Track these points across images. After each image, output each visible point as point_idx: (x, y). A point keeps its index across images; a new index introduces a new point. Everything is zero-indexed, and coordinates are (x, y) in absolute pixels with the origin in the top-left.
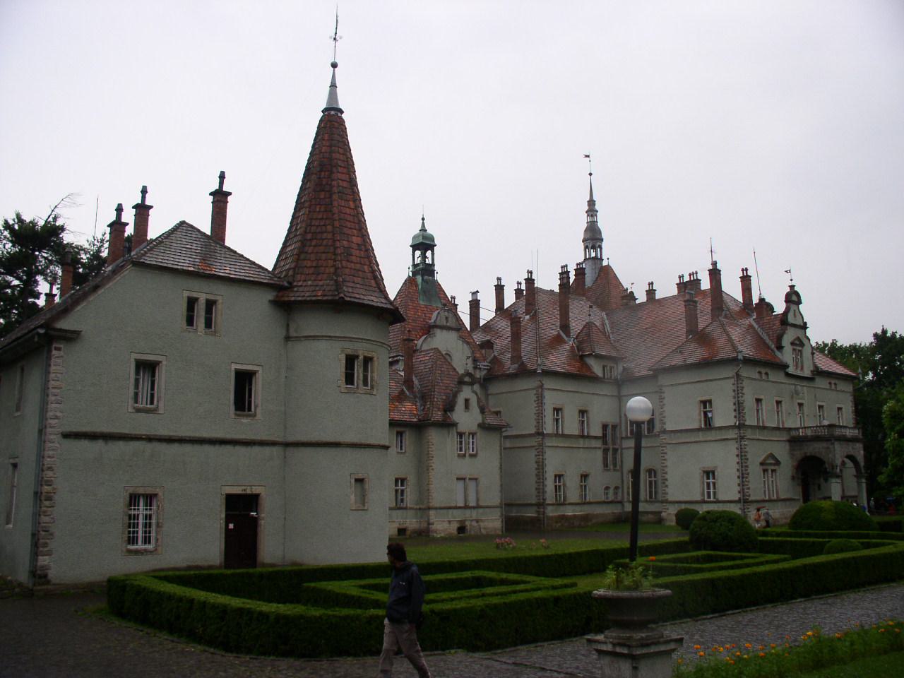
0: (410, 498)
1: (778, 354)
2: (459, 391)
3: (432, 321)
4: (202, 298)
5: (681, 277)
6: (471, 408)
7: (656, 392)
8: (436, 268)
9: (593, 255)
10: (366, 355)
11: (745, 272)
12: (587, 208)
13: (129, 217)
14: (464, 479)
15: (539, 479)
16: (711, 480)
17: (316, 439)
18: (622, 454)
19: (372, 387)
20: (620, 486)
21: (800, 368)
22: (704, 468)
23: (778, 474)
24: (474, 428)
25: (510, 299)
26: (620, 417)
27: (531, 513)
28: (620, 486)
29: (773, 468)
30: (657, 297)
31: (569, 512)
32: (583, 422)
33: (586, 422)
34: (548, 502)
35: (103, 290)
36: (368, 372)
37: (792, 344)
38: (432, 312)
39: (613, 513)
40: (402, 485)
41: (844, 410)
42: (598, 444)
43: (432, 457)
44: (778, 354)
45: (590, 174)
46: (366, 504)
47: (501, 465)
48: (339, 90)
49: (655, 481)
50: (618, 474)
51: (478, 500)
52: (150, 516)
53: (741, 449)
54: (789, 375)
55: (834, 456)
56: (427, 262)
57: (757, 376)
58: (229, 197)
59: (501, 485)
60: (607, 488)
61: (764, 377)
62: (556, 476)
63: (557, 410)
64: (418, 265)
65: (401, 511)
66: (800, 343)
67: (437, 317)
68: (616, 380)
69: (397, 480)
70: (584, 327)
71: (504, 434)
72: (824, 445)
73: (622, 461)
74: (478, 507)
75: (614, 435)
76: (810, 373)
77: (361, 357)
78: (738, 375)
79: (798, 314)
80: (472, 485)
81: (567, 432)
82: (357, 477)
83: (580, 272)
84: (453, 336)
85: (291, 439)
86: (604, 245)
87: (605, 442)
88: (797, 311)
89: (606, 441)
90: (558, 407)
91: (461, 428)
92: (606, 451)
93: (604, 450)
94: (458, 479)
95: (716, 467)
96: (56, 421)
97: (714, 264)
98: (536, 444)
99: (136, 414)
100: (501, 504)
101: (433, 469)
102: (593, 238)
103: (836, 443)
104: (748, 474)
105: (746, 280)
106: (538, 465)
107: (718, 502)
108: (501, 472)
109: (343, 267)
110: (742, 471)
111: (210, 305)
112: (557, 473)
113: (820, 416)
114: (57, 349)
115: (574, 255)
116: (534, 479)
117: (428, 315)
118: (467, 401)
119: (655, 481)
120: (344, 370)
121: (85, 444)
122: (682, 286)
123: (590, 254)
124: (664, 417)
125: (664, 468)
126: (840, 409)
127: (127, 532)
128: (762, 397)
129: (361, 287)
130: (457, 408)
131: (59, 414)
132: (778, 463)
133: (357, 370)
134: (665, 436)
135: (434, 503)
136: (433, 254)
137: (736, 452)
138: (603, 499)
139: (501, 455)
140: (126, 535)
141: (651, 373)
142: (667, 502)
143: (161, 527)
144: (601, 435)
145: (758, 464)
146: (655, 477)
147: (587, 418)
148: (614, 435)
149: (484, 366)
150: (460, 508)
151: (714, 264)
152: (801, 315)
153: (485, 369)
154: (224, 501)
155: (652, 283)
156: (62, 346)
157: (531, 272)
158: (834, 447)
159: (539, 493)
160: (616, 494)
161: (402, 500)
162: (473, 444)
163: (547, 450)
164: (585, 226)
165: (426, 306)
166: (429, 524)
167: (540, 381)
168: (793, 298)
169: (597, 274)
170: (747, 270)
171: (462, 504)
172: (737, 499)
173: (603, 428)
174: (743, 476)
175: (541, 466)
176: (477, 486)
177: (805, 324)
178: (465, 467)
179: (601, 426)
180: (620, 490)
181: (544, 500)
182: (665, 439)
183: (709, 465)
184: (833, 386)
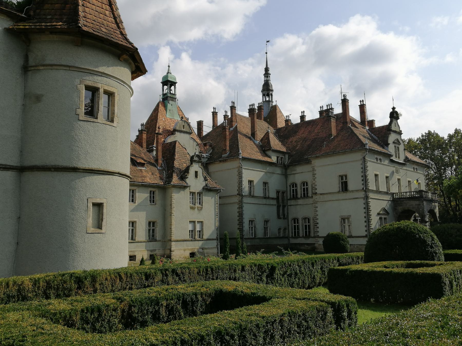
7: (309, 172)
9: (267, 99)
11: (362, 102)
12: (264, 72)
14: (194, 222)
15: (240, 222)
17: (53, 164)
18: (288, 209)
20: (287, 228)
21: (397, 157)
22: (342, 216)
28: (287, 228)
29: (385, 216)
32: (265, 189)
37: (394, 142)
40: (153, 226)
42: (275, 202)
45: (266, 53)
49: (309, 226)
50: (286, 220)
55: (423, 210)
60: (279, 229)
62: (250, 221)
63: (250, 182)
64: (166, 94)
65: (152, 243)
66: (397, 142)
69: (150, 223)
70: (266, 134)
72: (417, 202)
73: (288, 213)
76: (403, 160)
81: (256, 194)
83: (260, 108)
84: (187, 136)
85: (28, 163)
86: (274, 94)
87: (278, 202)
90: (251, 179)
91: (192, 190)
93: (277, 206)
100: (217, 238)
105: (362, 107)
107: (351, 237)
110: (368, 218)
116: (238, 222)
118: (196, 172)
122: (321, 113)
123: (266, 99)
124: (316, 185)
125: (317, 217)
128: (377, 173)
129: (102, 25)
136: (175, 88)
137: (364, 206)
142: (318, 237)
144: (275, 197)
147: (268, 187)
152: (399, 126)
155: (304, 112)
157: (234, 103)
158: (423, 204)
160: (284, 232)
161: (153, 236)
162: (200, 200)
163: (244, 205)
164: (263, 83)
165: (171, 119)
166: (171, 251)
168: (394, 115)
170: (363, 101)
172: (365, 235)
173: (277, 193)
175: (241, 215)
177: (401, 131)
180: (287, 230)
182: (316, 199)
183: (345, 214)
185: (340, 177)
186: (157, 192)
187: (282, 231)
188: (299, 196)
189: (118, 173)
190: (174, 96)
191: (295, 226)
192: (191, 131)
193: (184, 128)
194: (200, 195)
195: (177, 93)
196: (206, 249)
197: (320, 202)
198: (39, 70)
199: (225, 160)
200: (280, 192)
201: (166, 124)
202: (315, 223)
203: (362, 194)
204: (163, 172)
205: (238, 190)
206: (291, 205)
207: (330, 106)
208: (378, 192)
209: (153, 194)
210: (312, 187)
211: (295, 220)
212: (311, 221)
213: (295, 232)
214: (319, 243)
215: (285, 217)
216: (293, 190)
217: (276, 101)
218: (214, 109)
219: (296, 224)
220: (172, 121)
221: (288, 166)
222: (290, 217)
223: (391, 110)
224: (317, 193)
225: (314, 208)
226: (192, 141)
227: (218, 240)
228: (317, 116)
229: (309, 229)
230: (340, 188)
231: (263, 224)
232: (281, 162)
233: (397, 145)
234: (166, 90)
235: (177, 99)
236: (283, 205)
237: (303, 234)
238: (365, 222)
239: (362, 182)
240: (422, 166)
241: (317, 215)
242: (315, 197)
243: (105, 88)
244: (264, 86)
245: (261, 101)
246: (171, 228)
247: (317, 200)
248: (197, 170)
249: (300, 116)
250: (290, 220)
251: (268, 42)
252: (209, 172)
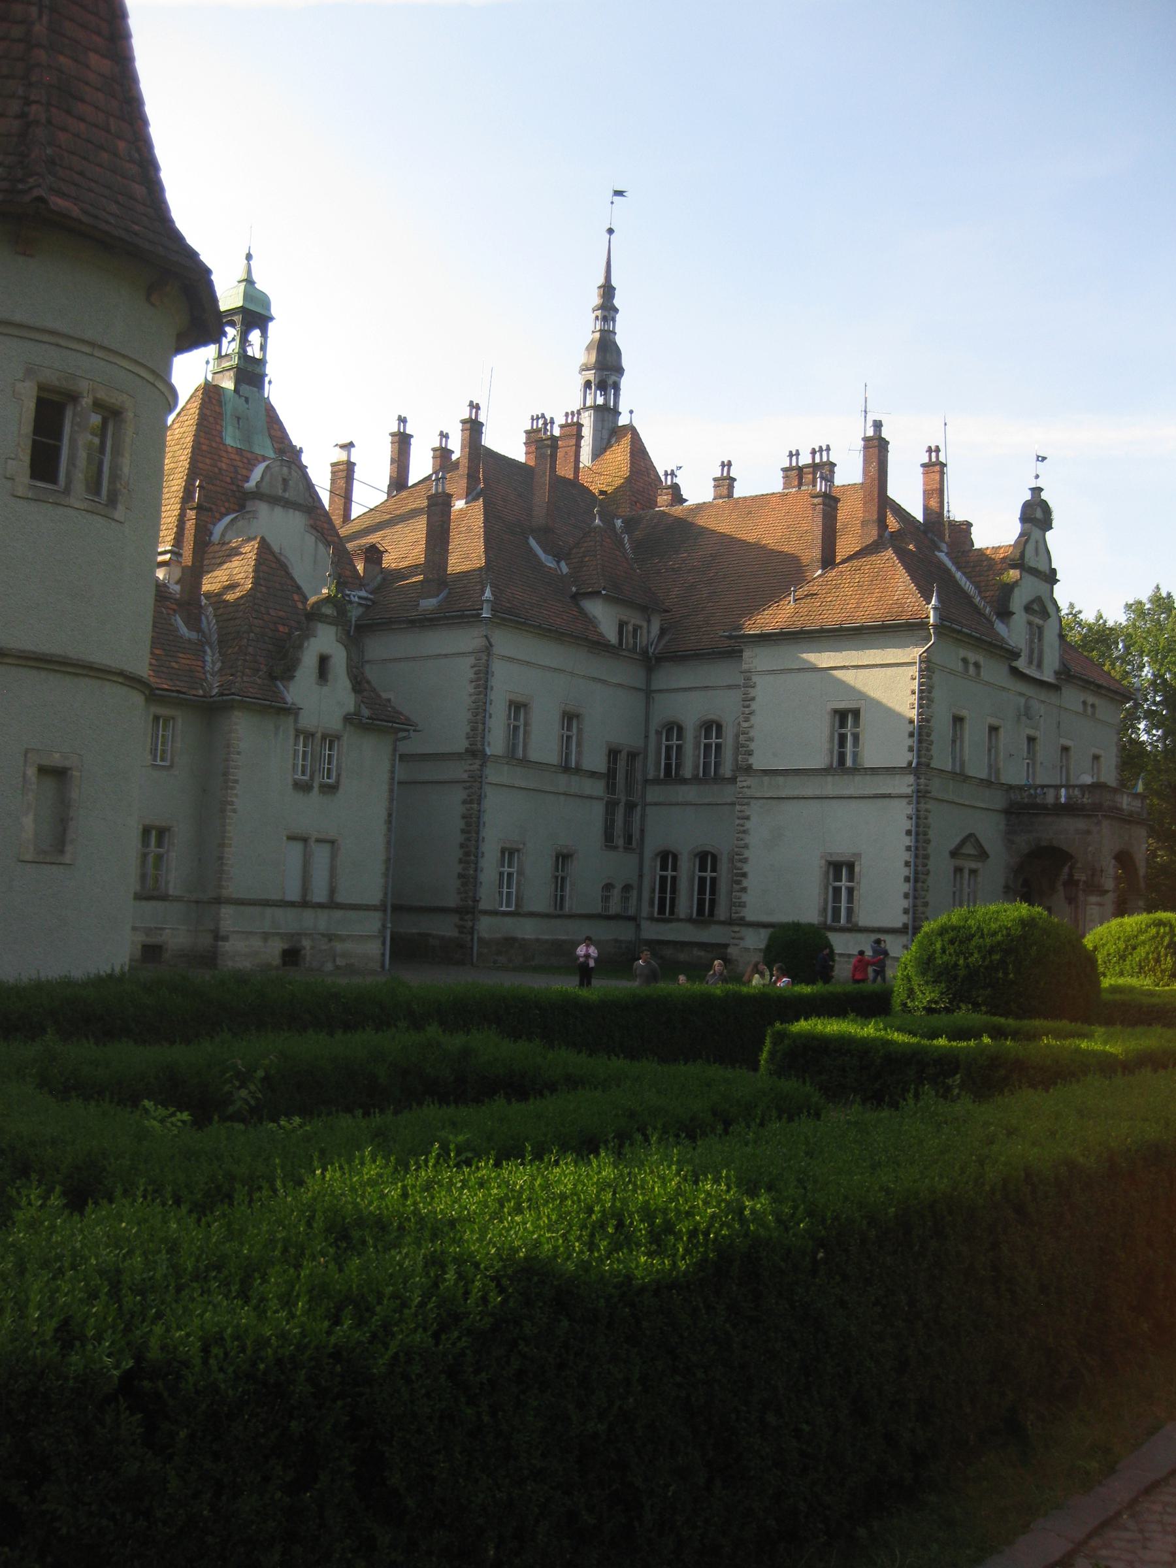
0: (175, 879)
1: (1000, 627)
2: (307, 634)
3: (251, 484)
6: (330, 677)
8: (270, 369)
9: (600, 401)
10: (101, 395)
11: (934, 454)
12: (596, 300)
14: (305, 840)
15: (467, 854)
16: (844, 883)
18: (643, 816)
19: (112, 501)
21: (1035, 662)
22: (831, 854)
24: (334, 723)
25: (421, 467)
26: (647, 737)
27: (445, 928)
30: (738, 493)
31: (527, 930)
32: (569, 738)
33: (574, 739)
34: (483, 905)
37: (1028, 609)
38: (250, 465)
39: (616, 941)
40: (160, 844)
42: (597, 788)
43: (236, 781)
44: (1000, 627)
45: (610, 231)
46: (69, 848)
47: (390, 815)
51: (332, 891)
53: (918, 818)
54: (1016, 672)
57: (960, 666)
59: (388, 860)
60: (608, 887)
61: (972, 669)
62: (503, 852)
63: (518, 707)
65: (153, 903)
67: (262, 478)
68: (645, 652)
69: (146, 831)
71: (406, 747)
72: (1080, 824)
73: (642, 831)
74: (332, 905)
75: (629, 775)
76: (1052, 674)
79: (1042, 551)
80: (321, 855)
81: (534, 756)
82: (45, 762)
86: (625, 383)
87: (611, 788)
88: (1041, 541)
89: (614, 784)
90: (520, 699)
91: (307, 721)
92: (611, 807)
93: (607, 802)
94: (291, 838)
95: (859, 855)
97: (878, 425)
98: (465, 776)
101: (234, 811)
103: (1105, 823)
104: (927, 873)
106: (468, 824)
108: (389, 830)
109: (49, 122)
110: (916, 866)
112: (508, 845)
113: (1061, 767)
117: (244, 472)
118: (323, 661)
119: (713, 880)
120: (28, 428)
126: (1096, 758)
128: (964, 713)
130: (298, 674)
132: (983, 855)
134: (749, 781)
135: (232, 889)
137: (908, 825)
138: (598, 908)
139: (391, 791)
142: (743, 923)
145: (947, 855)
146: (714, 870)
147: (580, 730)
148: (629, 775)
149: (360, 598)
150: (292, 904)
153: (360, 604)
155: (729, 464)
157: (478, 407)
159: (464, 884)
160: (625, 899)
163: (488, 790)
165: (239, 451)
166: (217, 936)
167: (486, 636)
169: (605, 441)
170: (938, 450)
171: (294, 895)
172: (899, 925)
174: (918, 877)
175: (472, 826)
176: (333, 857)
177: (1054, 571)
179: (605, 751)
180: (635, 893)
181: (476, 901)
183: (842, 849)
184: (1089, 709)
185: (837, 718)
186: (180, 721)
187: (616, 893)
188: (687, 772)
189: (121, 673)
190: (257, 371)
191: (663, 879)
192: (311, 500)
193: (285, 490)
194: (331, 743)
195: (268, 358)
196: (342, 939)
197: (761, 801)
199: (431, 620)
200: (620, 752)
201: (220, 469)
202: (737, 875)
203: (904, 785)
204: (205, 652)
205: (467, 734)
206: (656, 804)
207: (824, 453)
208: (960, 776)
210: (738, 747)
211: (668, 858)
212: (724, 866)
213: (662, 901)
214: (742, 944)
215: (631, 842)
216: (668, 748)
217: (631, 412)
218: (399, 424)
219: (670, 873)
220: (245, 461)
221: (656, 658)
222: (652, 846)
223: (1028, 496)
224: (754, 767)
225: (738, 822)
226: (310, 539)
227: (385, 911)
228: (774, 484)
229: (713, 892)
230: (832, 752)
231: (550, 863)
232: (635, 643)
234: (229, 342)
235: (267, 380)
236: (627, 800)
237: (691, 908)
238: (907, 879)
239: (910, 742)
240: (1112, 699)
241: (746, 846)
242: (743, 781)
243: (99, 396)
246: (221, 858)
247: (748, 792)
248: (326, 650)
249: (715, 480)
250: (648, 853)
251: (619, 193)
252: (366, 658)
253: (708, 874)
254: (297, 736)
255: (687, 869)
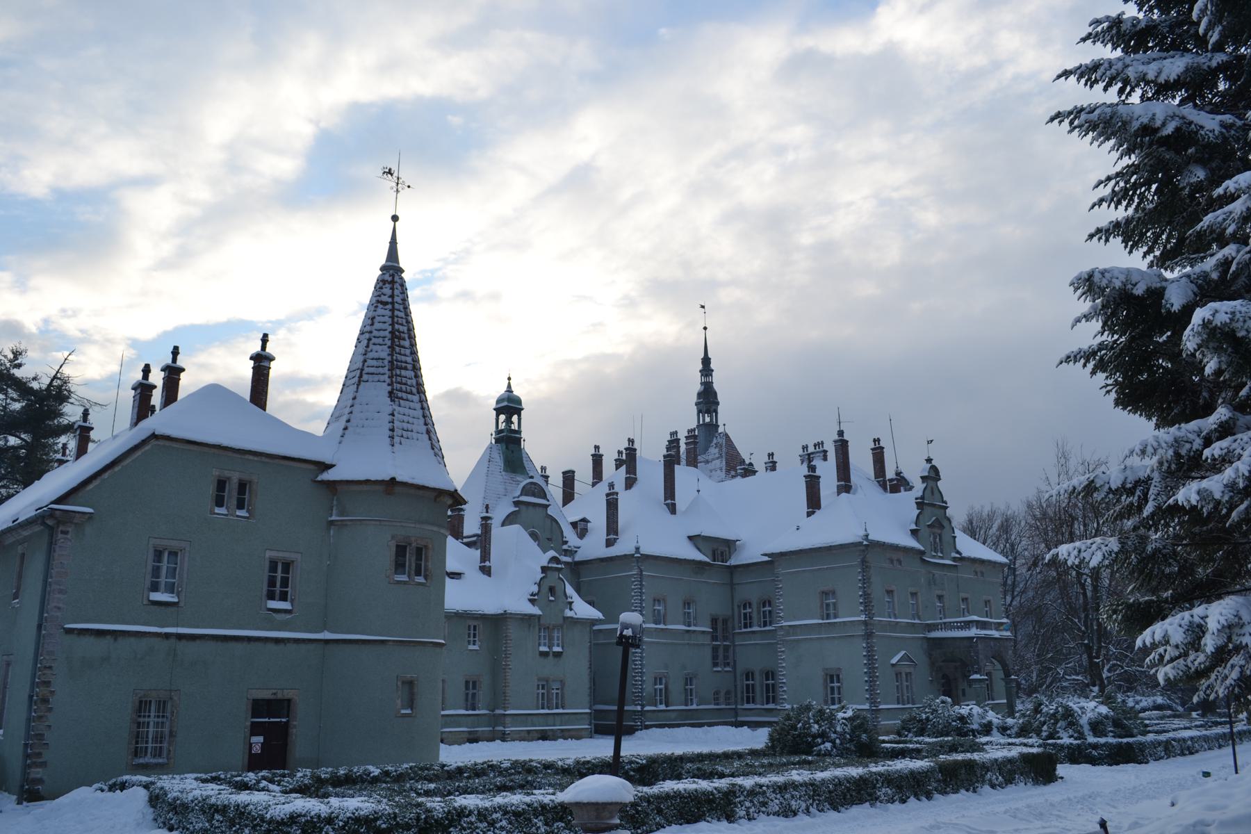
4: (235, 477)
5: (805, 448)
8: (523, 435)
9: (708, 420)
10: (419, 542)
12: (700, 367)
13: (157, 378)
22: (827, 669)
23: (913, 677)
26: (733, 609)
35: (120, 467)
36: (421, 560)
40: (474, 687)
41: (992, 601)
42: (707, 640)
45: (705, 328)
48: (399, 246)
52: (163, 723)
56: (513, 428)
58: (272, 363)
60: (717, 693)
64: (502, 431)
69: (467, 682)
77: (414, 545)
78: (864, 561)
79: (936, 492)
86: (720, 409)
96: (59, 614)
97: (841, 433)
99: (152, 607)
102: (708, 399)
105: (878, 454)
111: (242, 486)
114: (62, 532)
115: (686, 419)
120: (393, 558)
121: (91, 640)
123: (704, 420)
127: (134, 742)
128: (893, 588)
131: (61, 605)
133: (410, 560)
139: (590, 652)
140: (133, 746)
141: (766, 559)
143: (175, 736)
151: (841, 433)
152: (941, 493)
154: (250, 707)
155: (773, 454)
156: (70, 529)
170: (879, 440)
178: (548, 668)
195: (522, 429)
198: (346, 525)
203: (860, 631)
209: (475, 630)
211: (749, 675)
216: (745, 614)
226: (548, 522)
233: (937, 531)
244: (699, 395)
245: (694, 425)
246: (504, 693)
253: (770, 682)
254: (540, 629)
255: (758, 681)
